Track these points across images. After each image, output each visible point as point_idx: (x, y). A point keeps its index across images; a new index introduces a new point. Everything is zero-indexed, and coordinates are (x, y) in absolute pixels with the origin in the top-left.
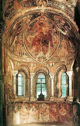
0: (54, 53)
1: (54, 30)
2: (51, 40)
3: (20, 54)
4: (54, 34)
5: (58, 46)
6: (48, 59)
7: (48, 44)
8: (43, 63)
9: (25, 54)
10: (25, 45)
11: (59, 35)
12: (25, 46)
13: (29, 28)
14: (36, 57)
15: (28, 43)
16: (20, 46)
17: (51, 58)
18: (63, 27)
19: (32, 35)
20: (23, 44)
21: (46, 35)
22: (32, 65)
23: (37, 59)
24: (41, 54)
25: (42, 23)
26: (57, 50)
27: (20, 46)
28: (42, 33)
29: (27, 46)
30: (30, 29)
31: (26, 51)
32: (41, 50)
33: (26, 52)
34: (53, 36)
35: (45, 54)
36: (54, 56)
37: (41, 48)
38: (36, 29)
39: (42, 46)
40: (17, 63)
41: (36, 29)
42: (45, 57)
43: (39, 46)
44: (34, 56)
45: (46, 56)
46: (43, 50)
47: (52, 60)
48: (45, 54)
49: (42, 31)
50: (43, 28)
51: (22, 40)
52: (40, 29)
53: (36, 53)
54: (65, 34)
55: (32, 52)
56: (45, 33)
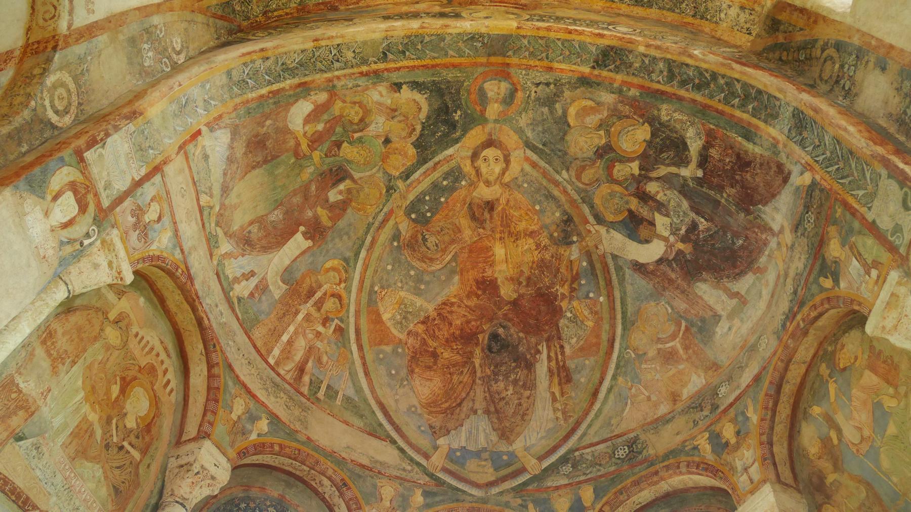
0: (578, 424)
1: (574, 252)
2: (555, 338)
3: (306, 379)
4: (573, 290)
5: (612, 366)
6: (534, 467)
7: (530, 366)
8: (495, 490)
9: (347, 399)
10: (360, 348)
11: (609, 283)
12: (354, 348)
13: (405, 227)
14: (436, 448)
15: (381, 336)
16: (320, 329)
17: (564, 460)
18: (634, 204)
19: (418, 292)
20: (340, 331)
21: (515, 303)
22: (388, 491)
23: (437, 460)
24: (476, 432)
25: (490, 206)
26: (602, 395)
27: (320, 329)
28: (488, 286)
29: (369, 357)
30: (413, 244)
31: (359, 390)
32: (480, 405)
33: (351, 392)
34: (564, 304)
35: (505, 435)
36: (587, 441)
37: (479, 392)
38: (454, 249)
39: (486, 380)
40: (253, 419)
41: (454, 249)
42: (512, 455)
43: (466, 378)
44: (411, 432)
45: (518, 446)
46: (495, 409)
47: (567, 469)
48: (505, 435)
49: (489, 273)
50: (499, 251)
51: (344, 295)
52: (479, 252)
53: (437, 421)
54: (651, 252)
55: (403, 406)
56: (507, 291)
